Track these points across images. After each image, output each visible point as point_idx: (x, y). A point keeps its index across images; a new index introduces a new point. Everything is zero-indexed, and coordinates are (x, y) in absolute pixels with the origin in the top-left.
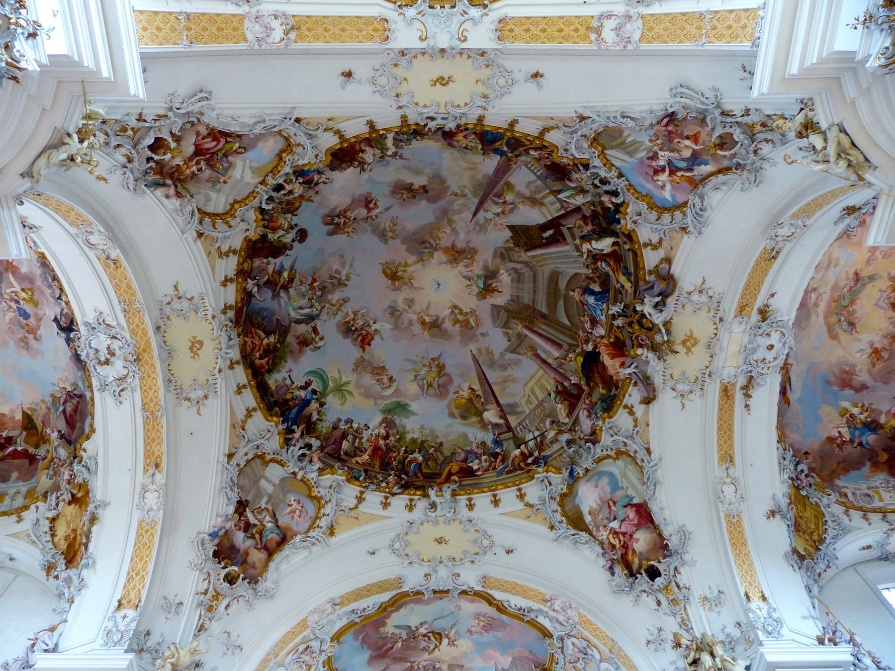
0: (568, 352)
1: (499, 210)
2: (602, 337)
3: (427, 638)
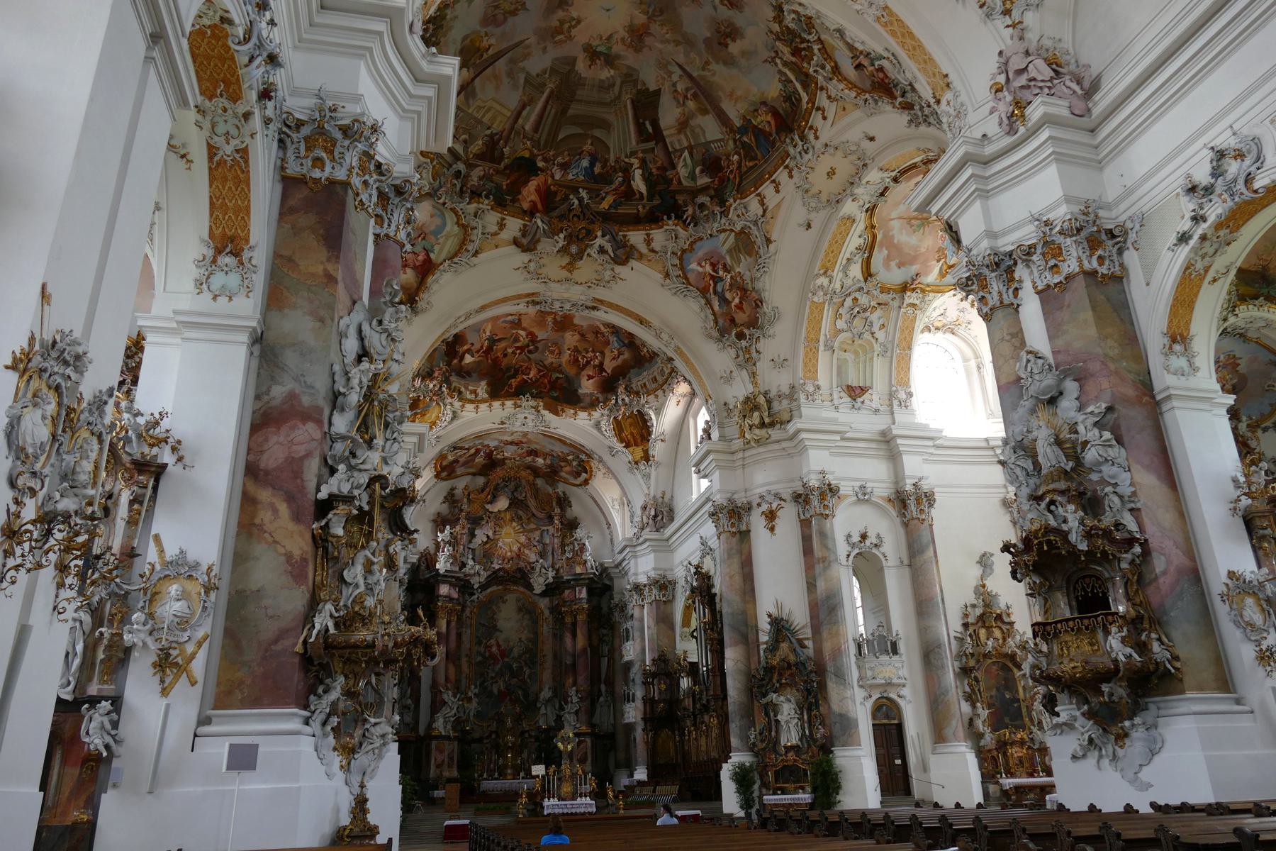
0: (531, 139)
1: (679, 90)
2: (553, 177)
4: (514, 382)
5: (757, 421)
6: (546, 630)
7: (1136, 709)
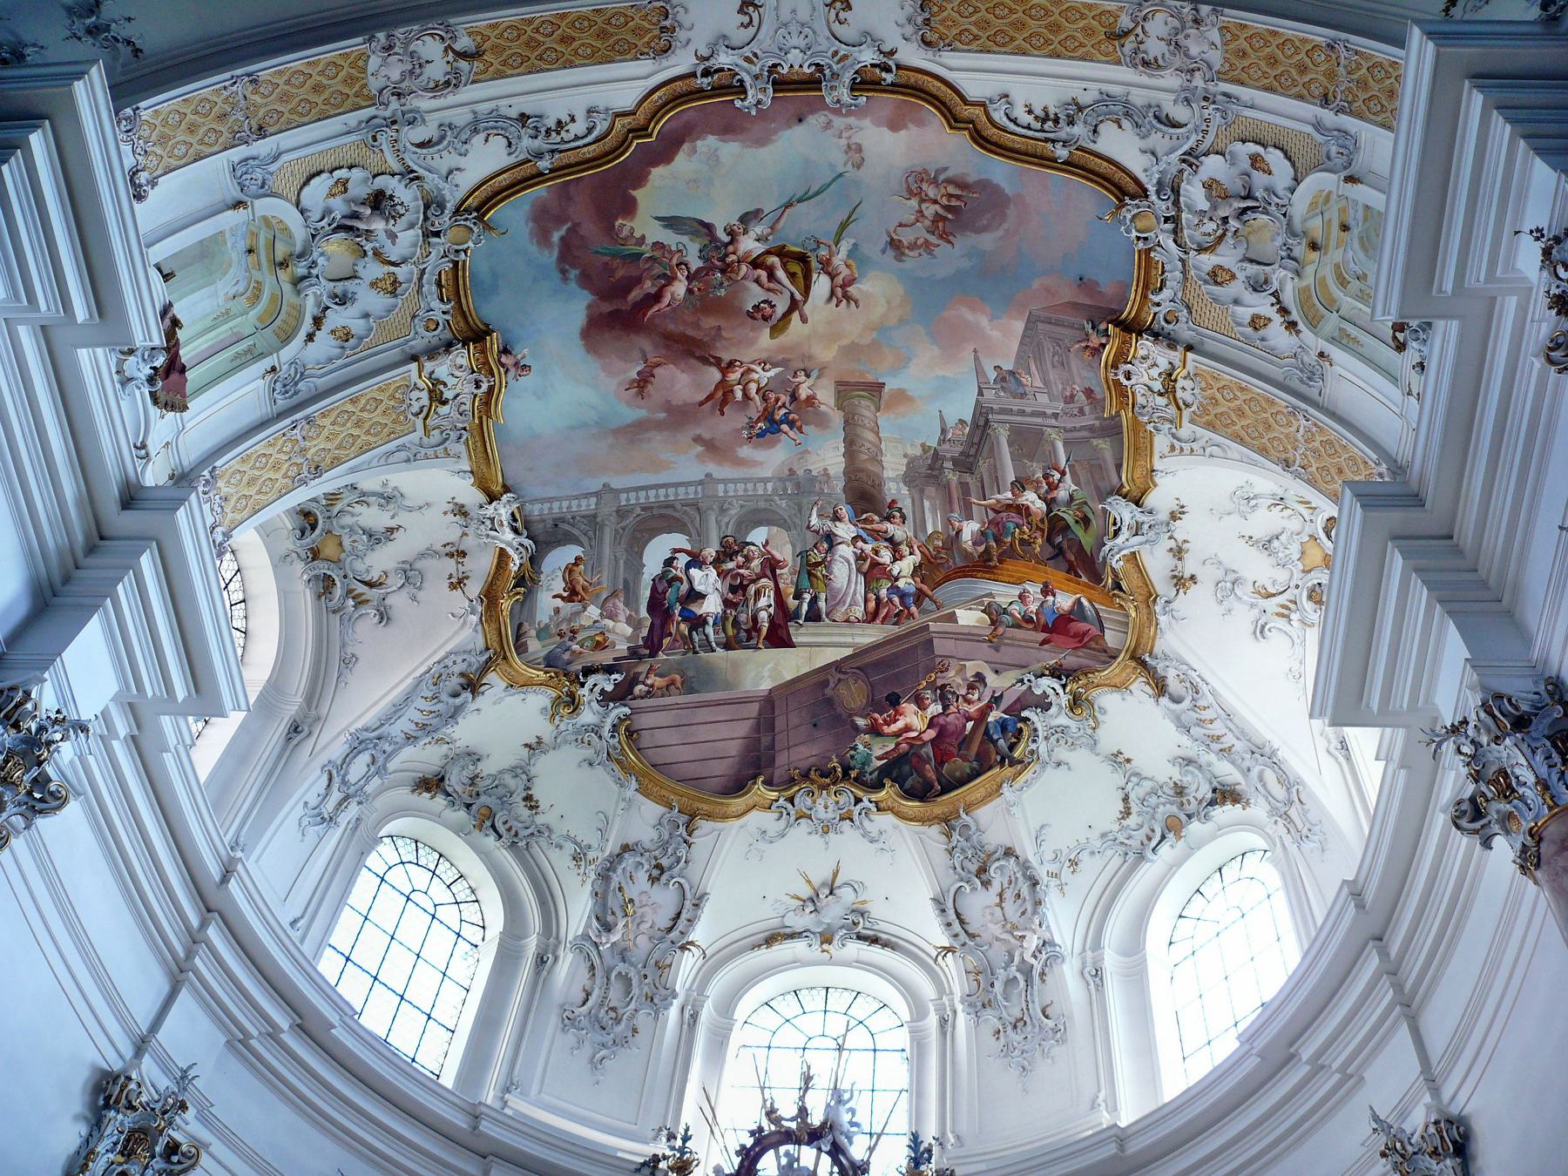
3: (763, 274)
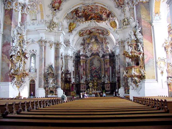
4: (90, 17)
5: (125, 24)
6: (103, 64)
7: (140, 82)
